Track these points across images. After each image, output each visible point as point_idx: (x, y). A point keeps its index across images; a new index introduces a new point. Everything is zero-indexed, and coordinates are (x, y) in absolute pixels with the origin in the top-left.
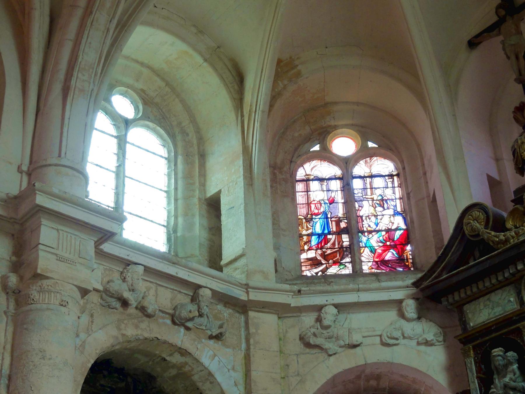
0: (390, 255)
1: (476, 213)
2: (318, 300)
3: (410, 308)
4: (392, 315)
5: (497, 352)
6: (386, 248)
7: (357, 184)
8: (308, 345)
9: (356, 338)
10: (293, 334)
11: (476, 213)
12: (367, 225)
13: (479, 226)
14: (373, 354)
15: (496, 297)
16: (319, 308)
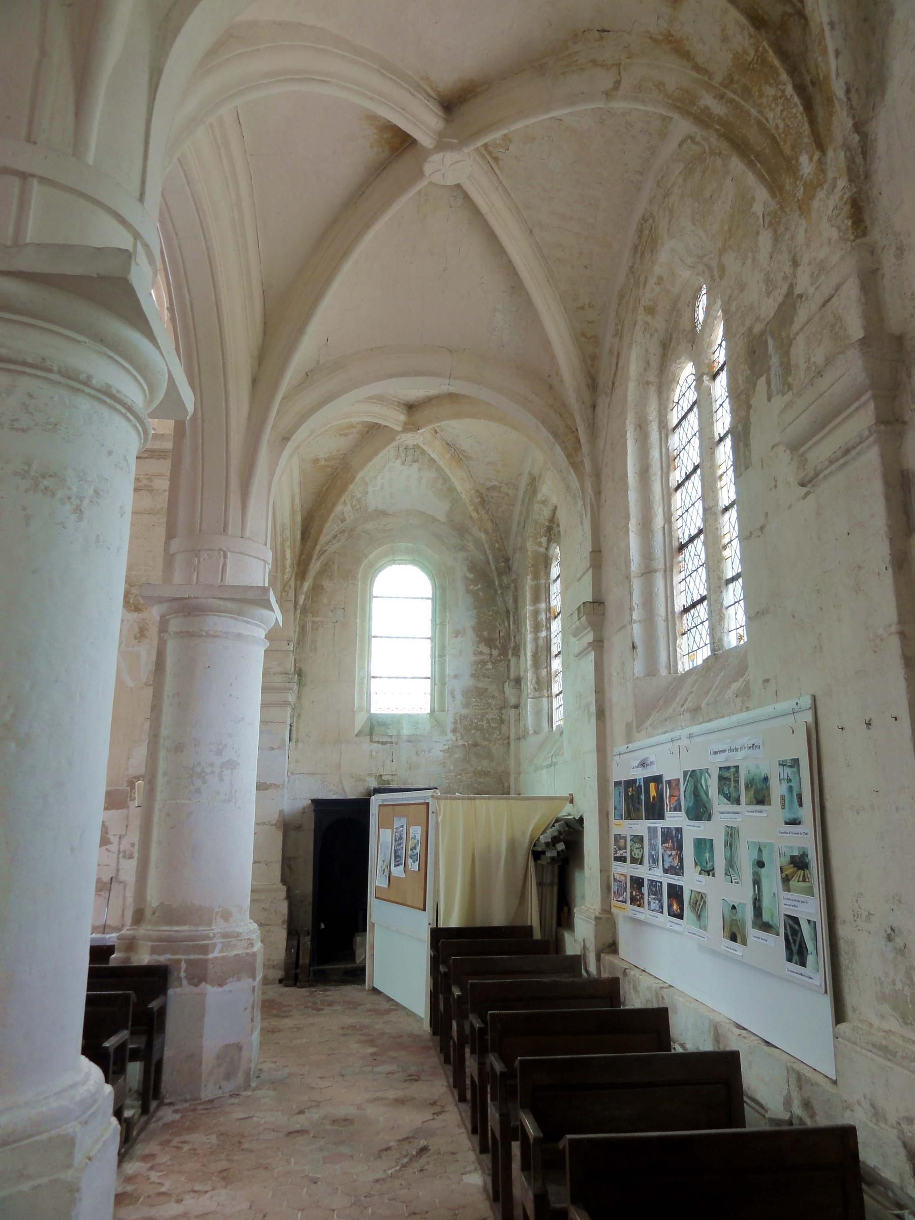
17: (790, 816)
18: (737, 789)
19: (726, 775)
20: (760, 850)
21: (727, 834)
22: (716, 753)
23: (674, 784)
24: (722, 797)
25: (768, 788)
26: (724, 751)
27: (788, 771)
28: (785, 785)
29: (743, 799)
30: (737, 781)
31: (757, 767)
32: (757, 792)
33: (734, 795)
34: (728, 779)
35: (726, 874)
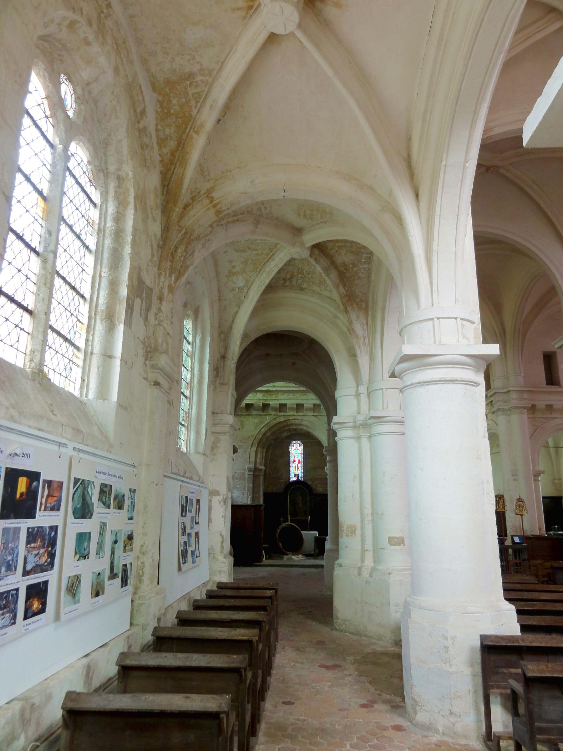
17: (130, 516)
18: (110, 498)
19: (105, 489)
20: (116, 534)
21: (101, 527)
22: (100, 472)
23: (55, 485)
24: (100, 503)
25: (124, 500)
26: (105, 474)
27: (132, 494)
28: (130, 500)
29: (112, 506)
30: (110, 494)
31: (121, 489)
32: (119, 503)
33: (108, 502)
34: (105, 492)
35: (97, 554)
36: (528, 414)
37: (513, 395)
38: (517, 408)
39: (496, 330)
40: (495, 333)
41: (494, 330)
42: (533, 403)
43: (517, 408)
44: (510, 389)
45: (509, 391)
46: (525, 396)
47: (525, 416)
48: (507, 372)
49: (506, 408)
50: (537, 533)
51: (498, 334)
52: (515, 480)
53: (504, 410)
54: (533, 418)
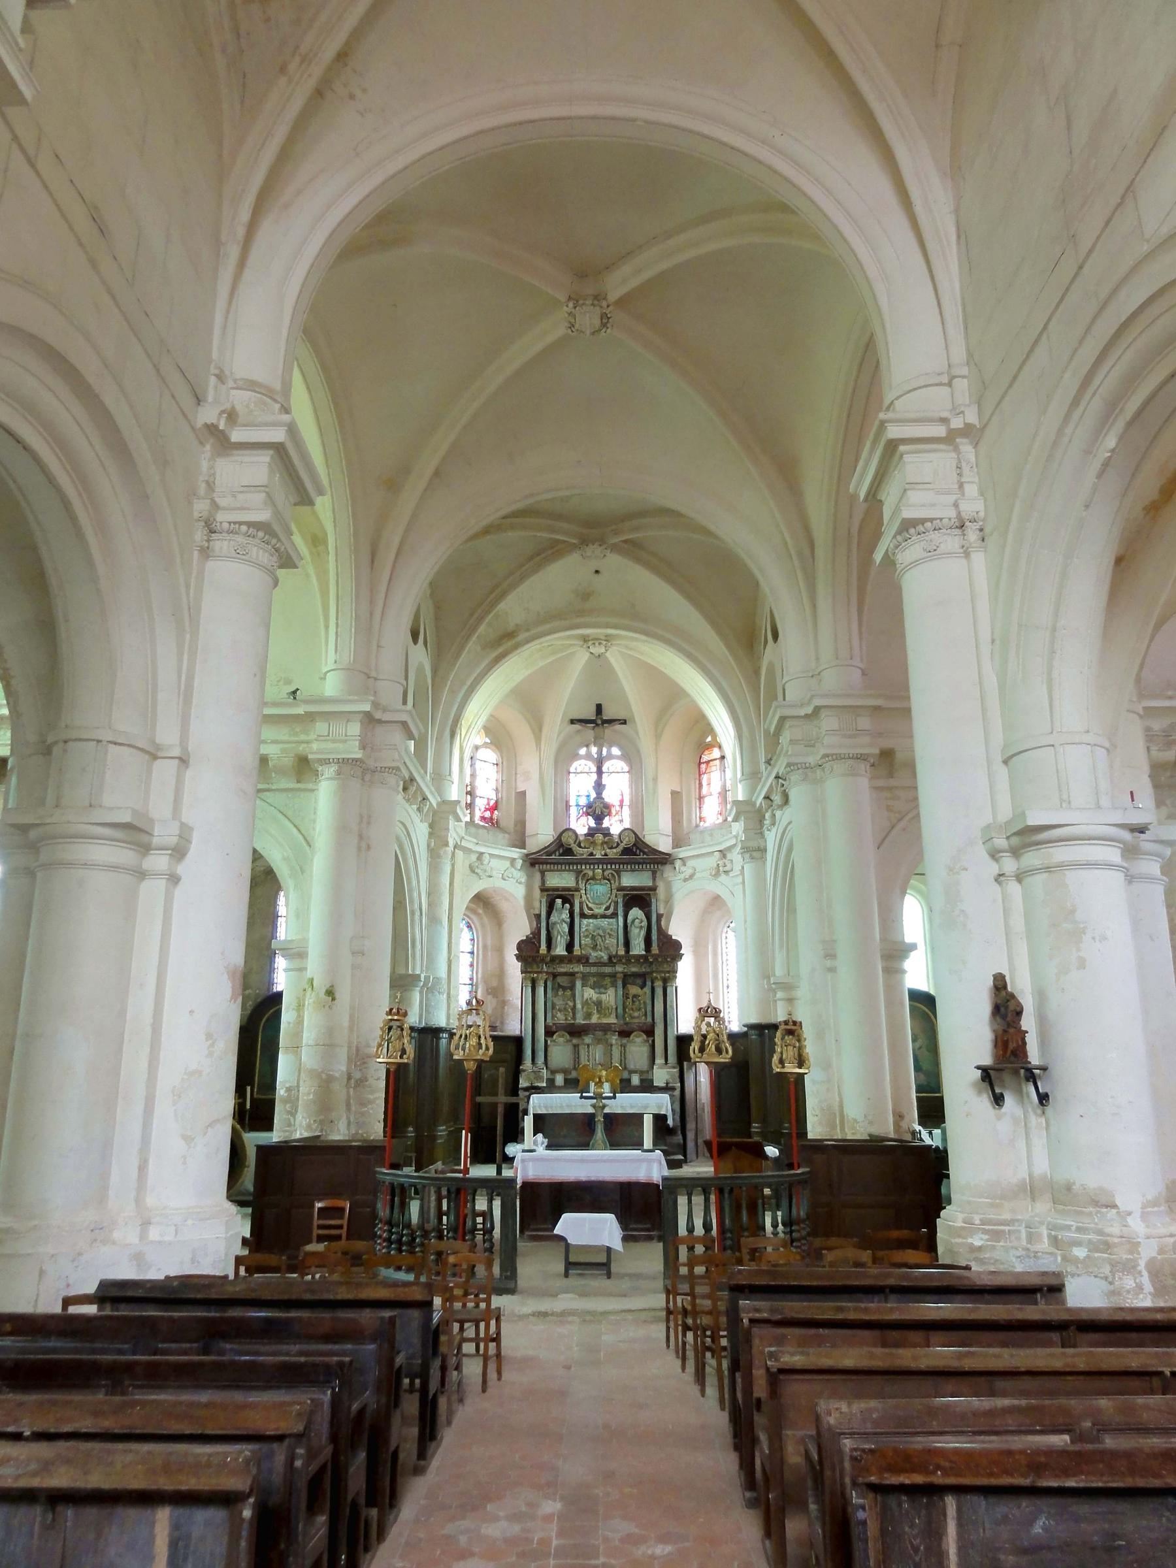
0: (488, 814)
1: (571, 833)
2: (482, 850)
3: (519, 863)
4: (507, 864)
5: (559, 901)
6: (486, 810)
7: (478, 765)
8: (473, 872)
9: (494, 873)
10: (467, 863)
11: (571, 833)
12: (478, 793)
13: (571, 841)
14: (498, 883)
15: (565, 874)
16: (482, 854)
36: (871, 779)
37: (828, 722)
38: (838, 757)
39: (788, 540)
40: (788, 549)
41: (786, 543)
42: (888, 744)
43: (838, 757)
44: (817, 702)
45: (817, 710)
46: (864, 723)
47: (864, 783)
48: (817, 659)
49: (812, 760)
50: (887, 1129)
51: (793, 552)
52: (832, 970)
53: (807, 767)
54: (890, 789)
